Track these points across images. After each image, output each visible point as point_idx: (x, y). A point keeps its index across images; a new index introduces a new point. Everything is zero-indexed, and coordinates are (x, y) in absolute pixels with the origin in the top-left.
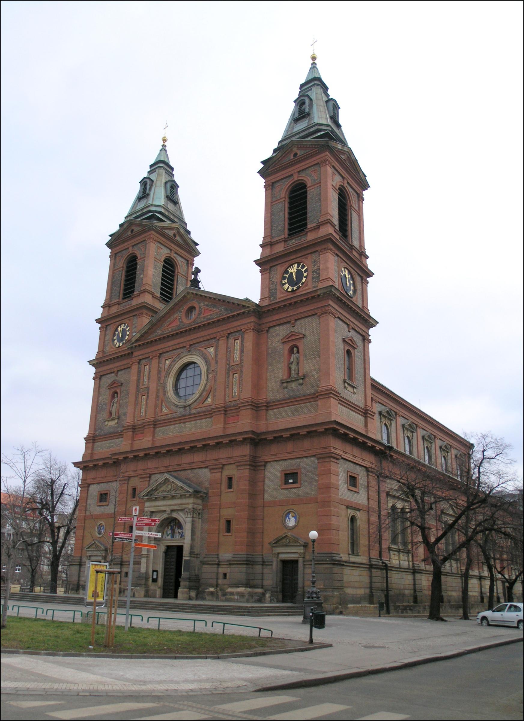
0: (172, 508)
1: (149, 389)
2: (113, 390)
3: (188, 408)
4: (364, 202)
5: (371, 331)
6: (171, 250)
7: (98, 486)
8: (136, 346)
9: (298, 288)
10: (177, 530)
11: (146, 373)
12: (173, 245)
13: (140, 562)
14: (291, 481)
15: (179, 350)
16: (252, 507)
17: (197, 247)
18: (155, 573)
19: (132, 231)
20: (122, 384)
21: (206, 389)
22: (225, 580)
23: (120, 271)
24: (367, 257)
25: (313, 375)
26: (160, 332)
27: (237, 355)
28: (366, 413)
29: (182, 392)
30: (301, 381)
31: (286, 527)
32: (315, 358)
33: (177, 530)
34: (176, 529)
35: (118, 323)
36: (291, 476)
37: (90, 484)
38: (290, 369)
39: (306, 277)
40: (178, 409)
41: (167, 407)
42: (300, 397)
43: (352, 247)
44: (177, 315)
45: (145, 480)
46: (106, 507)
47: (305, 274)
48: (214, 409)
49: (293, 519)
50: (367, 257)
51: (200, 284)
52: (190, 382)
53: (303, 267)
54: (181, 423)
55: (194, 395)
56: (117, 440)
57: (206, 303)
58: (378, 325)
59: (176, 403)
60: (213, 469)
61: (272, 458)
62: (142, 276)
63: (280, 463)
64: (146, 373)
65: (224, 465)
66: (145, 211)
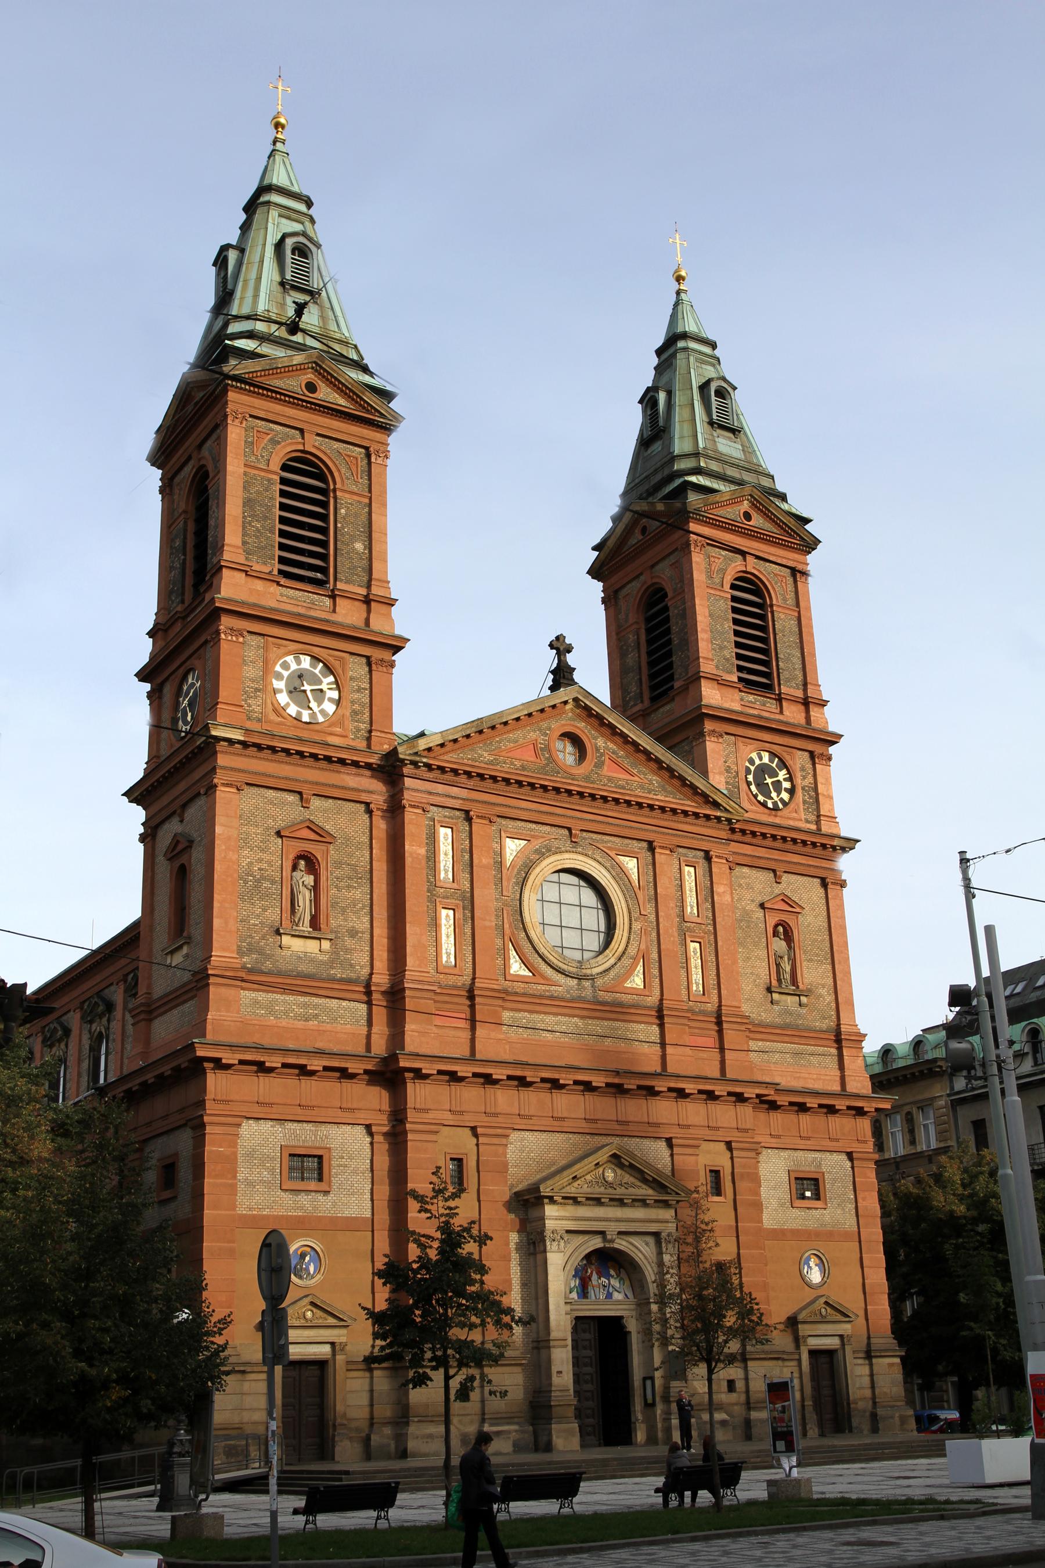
3: (587, 984)
7: (278, 1128)
15: (547, 828)
19: (311, 387)
21: (632, 951)
22: (734, 1395)
23: (269, 480)
25: (821, 996)
26: (487, 756)
27: (691, 899)
30: (804, 999)
31: (809, 1285)
34: (595, 1277)
38: (778, 965)
42: (800, 1030)
44: (533, 735)
46: (320, 1197)
57: (611, 745)
59: (556, 961)
61: (774, 1142)
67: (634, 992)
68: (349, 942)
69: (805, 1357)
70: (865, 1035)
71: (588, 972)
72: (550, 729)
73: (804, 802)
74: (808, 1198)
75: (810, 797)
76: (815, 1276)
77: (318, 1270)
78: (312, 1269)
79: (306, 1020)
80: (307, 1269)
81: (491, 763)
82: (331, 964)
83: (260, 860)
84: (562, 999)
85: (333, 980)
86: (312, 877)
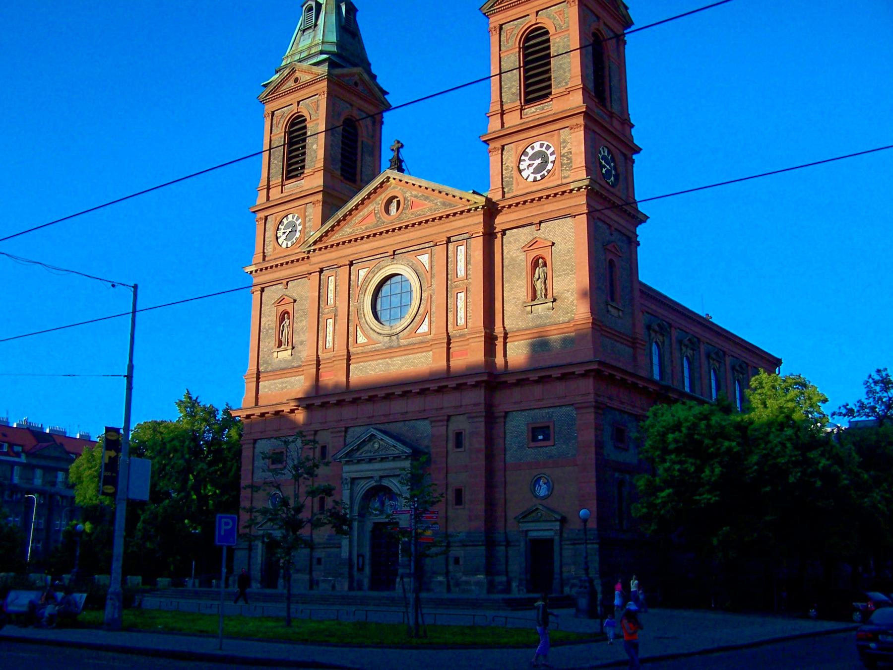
0: (381, 473)
1: (336, 310)
2: (281, 309)
3: (394, 338)
4: (626, 46)
5: (640, 230)
6: (351, 105)
8: (314, 250)
9: (543, 177)
10: (388, 503)
11: (331, 287)
12: (354, 98)
13: (340, 544)
14: (541, 437)
16: (490, 471)
17: (386, 97)
18: (361, 559)
19: (296, 80)
24: (632, 126)
26: (349, 230)
28: (633, 343)
29: (383, 316)
31: (537, 497)
32: (568, 274)
33: (388, 503)
35: (283, 214)
36: (540, 432)
37: (255, 441)
39: (553, 162)
40: (381, 337)
41: (366, 336)
43: (611, 115)
45: (339, 434)
47: (552, 158)
48: (433, 340)
49: (545, 486)
50: (632, 126)
51: (403, 164)
52: (395, 300)
53: (548, 147)
55: (403, 320)
58: (648, 221)
60: (435, 421)
61: (517, 407)
62: (315, 147)
63: (526, 413)
64: (331, 287)
65: (449, 417)
66: (313, 51)
67: (423, 334)
73: (562, 165)
75: (568, 159)
76: (542, 491)
81: (351, 233)
82: (292, 361)
84: (383, 350)
85: (293, 367)
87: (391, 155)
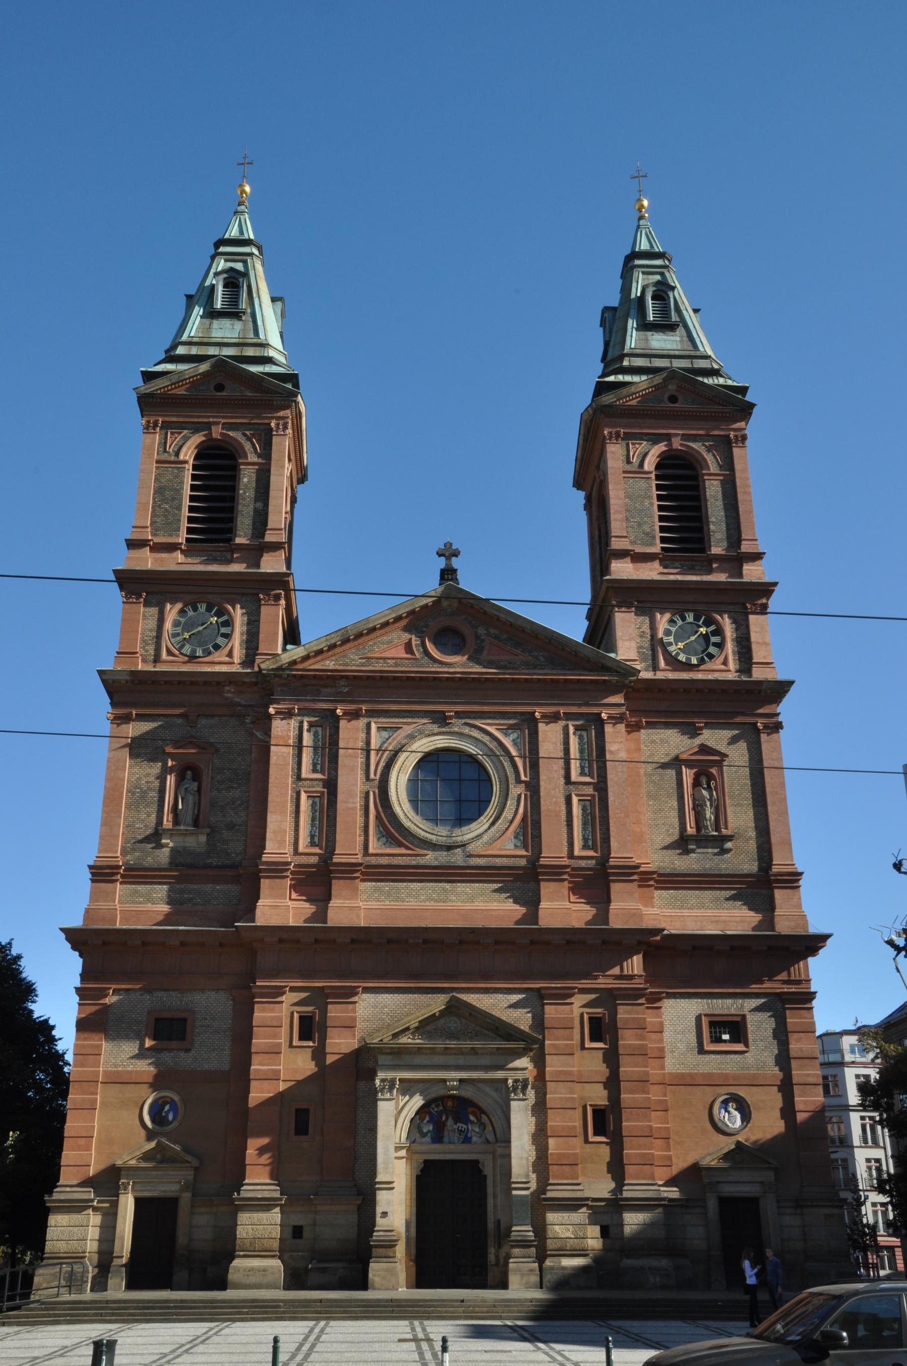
20: (217, 750)
54: (440, 881)
55: (473, 825)
56: (208, 887)
57: (492, 631)
68: (226, 834)
69: (712, 1204)
70: (801, 874)
71: (459, 839)
72: (426, 626)
74: (725, 1041)
77: (174, 1119)
78: (171, 1117)
79: (181, 904)
80: (167, 1116)
83: (148, 775)
86: (196, 784)
87: (442, 563)
